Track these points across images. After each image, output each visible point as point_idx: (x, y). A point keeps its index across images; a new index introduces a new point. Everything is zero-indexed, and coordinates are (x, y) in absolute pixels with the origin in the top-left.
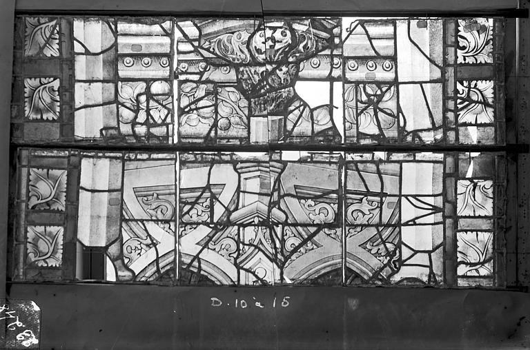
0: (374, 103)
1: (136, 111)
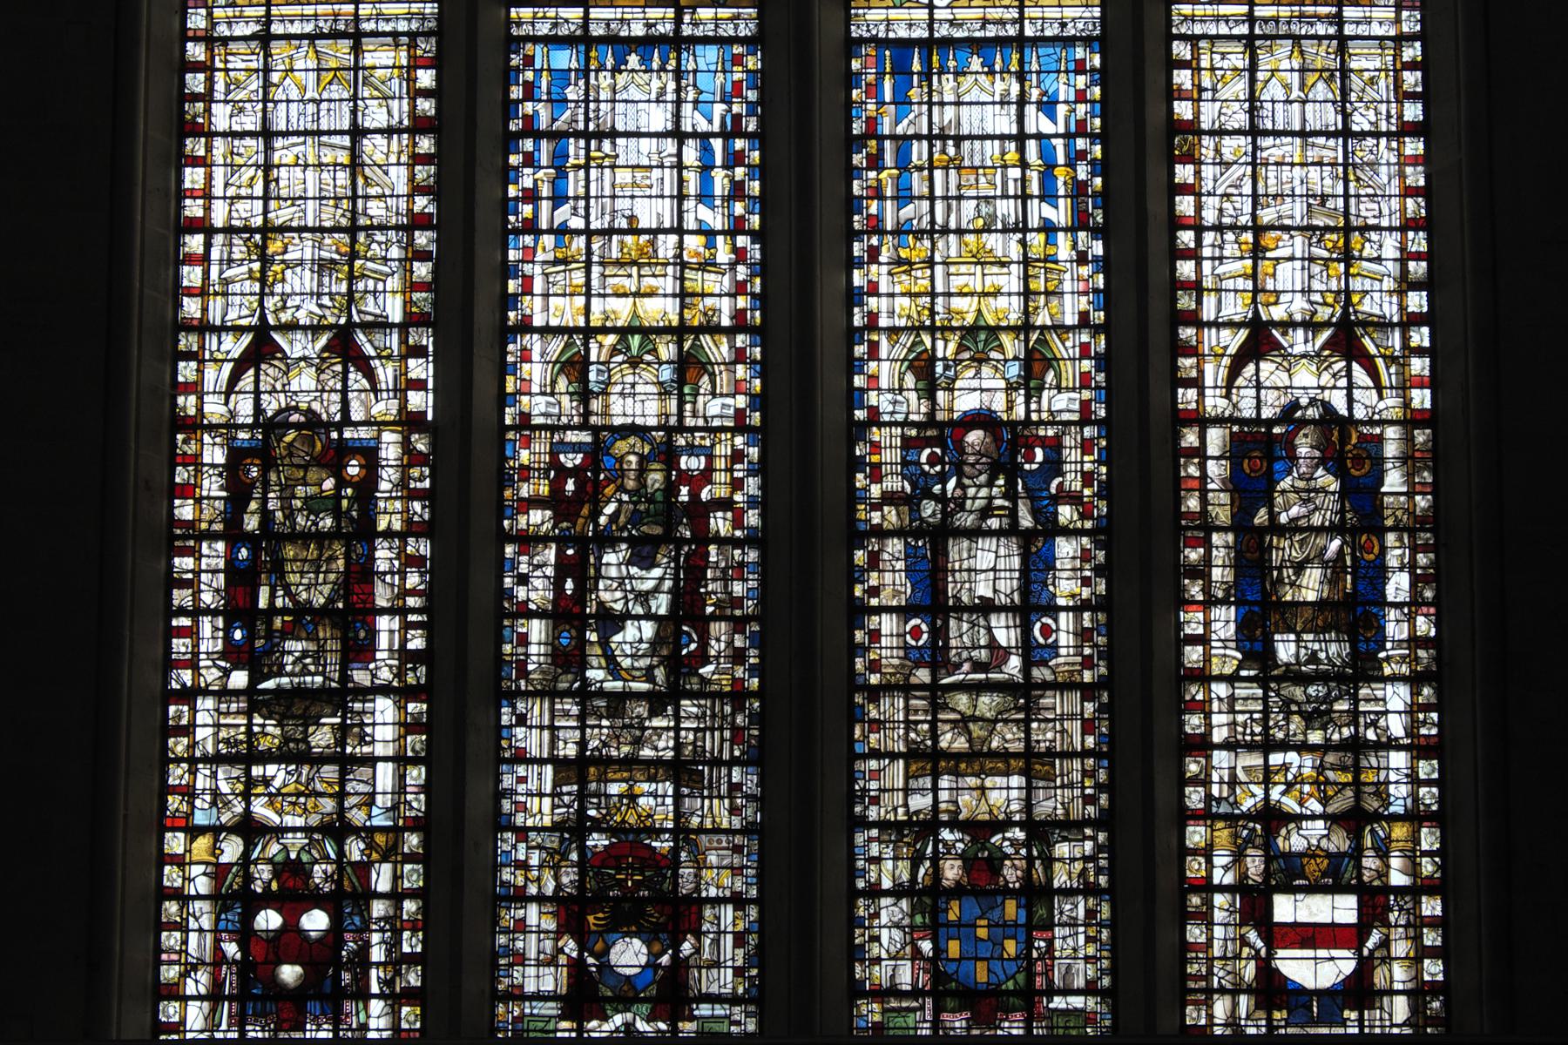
0: (1374, 724)
1: (1245, 729)
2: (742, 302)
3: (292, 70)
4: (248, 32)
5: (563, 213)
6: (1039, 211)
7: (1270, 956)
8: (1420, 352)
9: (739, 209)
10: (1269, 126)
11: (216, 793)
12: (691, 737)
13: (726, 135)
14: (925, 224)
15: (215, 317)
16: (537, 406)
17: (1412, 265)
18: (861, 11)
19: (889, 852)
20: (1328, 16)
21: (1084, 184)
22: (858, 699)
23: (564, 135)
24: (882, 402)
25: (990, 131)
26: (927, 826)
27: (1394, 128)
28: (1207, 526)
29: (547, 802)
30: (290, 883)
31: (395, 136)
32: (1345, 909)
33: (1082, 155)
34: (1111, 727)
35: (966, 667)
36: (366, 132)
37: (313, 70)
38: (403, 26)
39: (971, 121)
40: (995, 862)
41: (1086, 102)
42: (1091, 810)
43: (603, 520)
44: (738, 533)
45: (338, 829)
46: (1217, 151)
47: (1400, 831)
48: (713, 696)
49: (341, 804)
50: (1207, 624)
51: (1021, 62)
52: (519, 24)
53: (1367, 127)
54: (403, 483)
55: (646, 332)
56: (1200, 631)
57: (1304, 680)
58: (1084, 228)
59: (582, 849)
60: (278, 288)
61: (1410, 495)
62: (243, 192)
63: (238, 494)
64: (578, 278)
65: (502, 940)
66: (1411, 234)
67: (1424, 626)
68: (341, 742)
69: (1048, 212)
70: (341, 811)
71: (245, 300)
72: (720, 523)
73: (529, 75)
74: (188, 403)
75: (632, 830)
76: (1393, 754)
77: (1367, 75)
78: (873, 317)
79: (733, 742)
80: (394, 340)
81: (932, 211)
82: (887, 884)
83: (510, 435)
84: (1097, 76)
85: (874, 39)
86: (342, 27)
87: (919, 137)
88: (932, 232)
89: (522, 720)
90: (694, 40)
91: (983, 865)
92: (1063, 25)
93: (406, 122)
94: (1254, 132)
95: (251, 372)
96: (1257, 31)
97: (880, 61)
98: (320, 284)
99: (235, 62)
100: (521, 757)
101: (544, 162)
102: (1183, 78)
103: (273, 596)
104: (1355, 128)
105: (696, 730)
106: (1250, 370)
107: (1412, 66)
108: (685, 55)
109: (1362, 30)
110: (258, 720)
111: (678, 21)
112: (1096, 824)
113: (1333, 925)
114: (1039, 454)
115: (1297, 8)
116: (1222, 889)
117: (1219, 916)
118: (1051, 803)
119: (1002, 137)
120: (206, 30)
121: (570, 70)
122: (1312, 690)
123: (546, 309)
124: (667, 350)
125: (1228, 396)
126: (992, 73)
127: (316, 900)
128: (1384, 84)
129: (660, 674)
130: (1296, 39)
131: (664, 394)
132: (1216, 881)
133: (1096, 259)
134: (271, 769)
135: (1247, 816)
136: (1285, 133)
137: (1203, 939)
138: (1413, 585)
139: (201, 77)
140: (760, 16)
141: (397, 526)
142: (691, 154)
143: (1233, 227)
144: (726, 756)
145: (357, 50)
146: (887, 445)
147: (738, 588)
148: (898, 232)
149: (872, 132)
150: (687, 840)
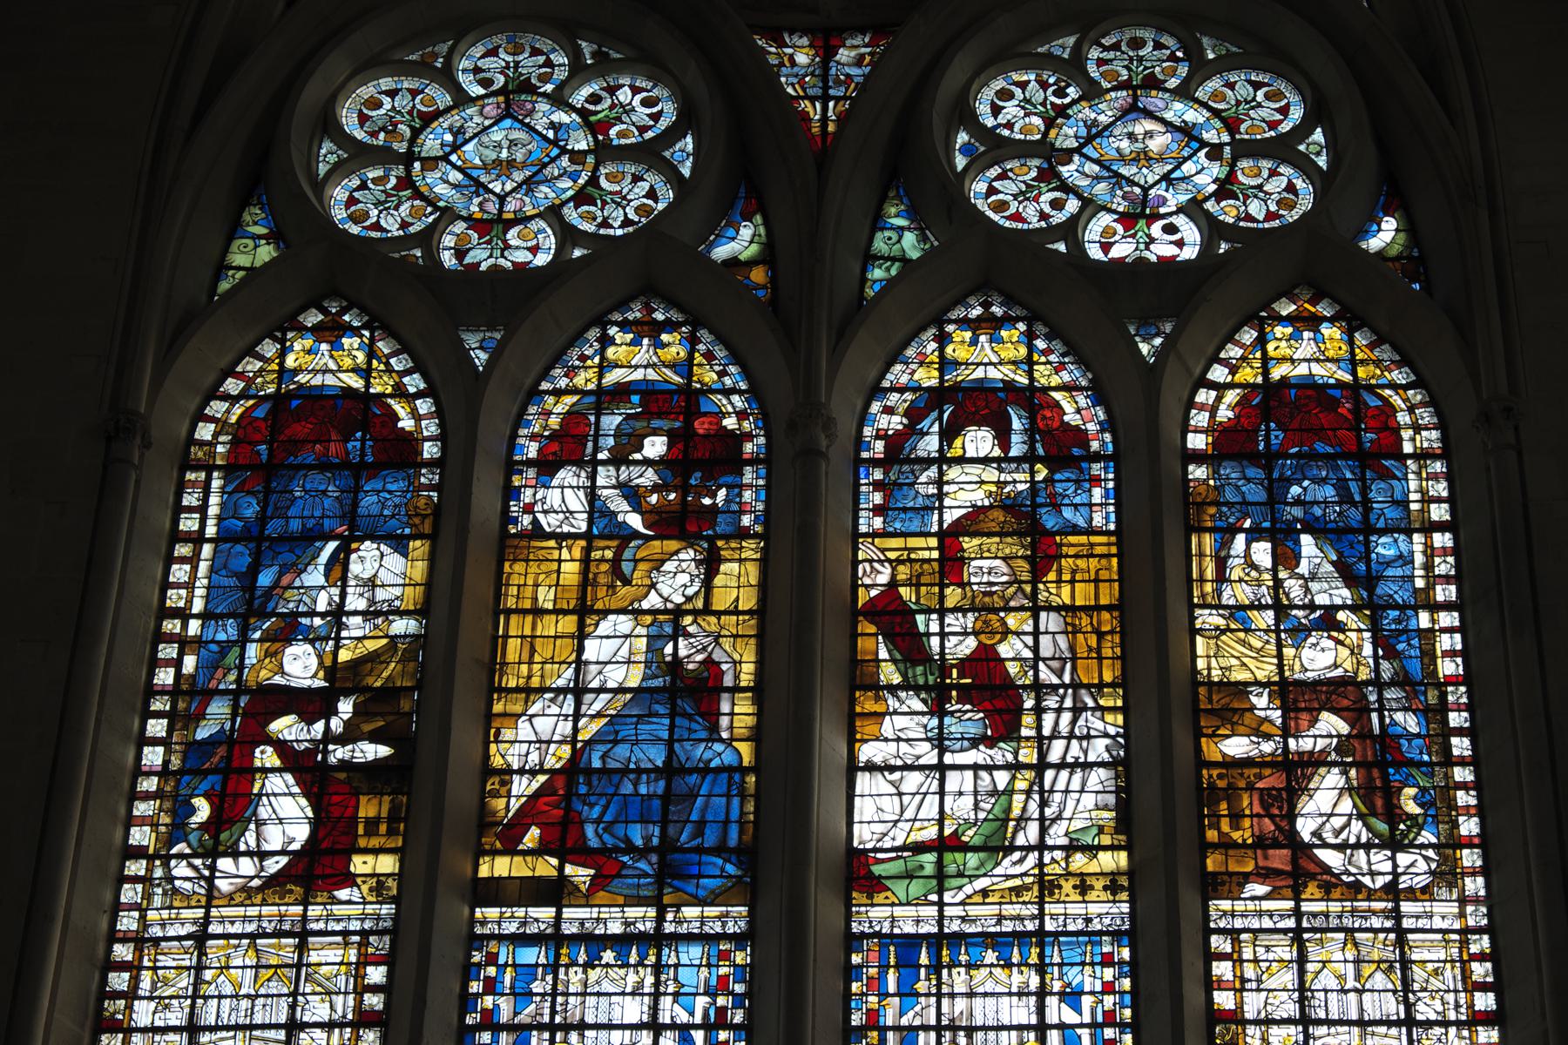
3: (228, 967)
4: (183, 932)
10: (1322, 1015)
13: (706, 1026)
18: (863, 909)
20: (1383, 911)
23: (529, 1027)
25: (1006, 1022)
27: (1464, 1018)
31: (337, 1031)
36: (304, 1026)
37: (251, 967)
38: (355, 925)
39: (983, 1012)
41: (1114, 992)
51: (1041, 956)
52: (484, 923)
53: (1433, 1017)
73: (492, 971)
77: (1430, 967)
84: (1126, 969)
85: (878, 935)
86: (287, 927)
87: (926, 1028)
90: (677, 938)
92: (1088, 920)
93: (350, 1016)
96: (1305, 924)
97: (883, 954)
99: (164, 961)
102: (1222, 969)
104: (1419, 1017)
107: (1481, 957)
108: (666, 951)
111: (660, 919)
115: (1349, 904)
119: (1020, 1028)
120: (137, 932)
121: (537, 965)
126: (1008, 965)
128: (1451, 975)
136: (1341, 1022)
139: (126, 976)
140: (751, 913)
145: (302, 948)
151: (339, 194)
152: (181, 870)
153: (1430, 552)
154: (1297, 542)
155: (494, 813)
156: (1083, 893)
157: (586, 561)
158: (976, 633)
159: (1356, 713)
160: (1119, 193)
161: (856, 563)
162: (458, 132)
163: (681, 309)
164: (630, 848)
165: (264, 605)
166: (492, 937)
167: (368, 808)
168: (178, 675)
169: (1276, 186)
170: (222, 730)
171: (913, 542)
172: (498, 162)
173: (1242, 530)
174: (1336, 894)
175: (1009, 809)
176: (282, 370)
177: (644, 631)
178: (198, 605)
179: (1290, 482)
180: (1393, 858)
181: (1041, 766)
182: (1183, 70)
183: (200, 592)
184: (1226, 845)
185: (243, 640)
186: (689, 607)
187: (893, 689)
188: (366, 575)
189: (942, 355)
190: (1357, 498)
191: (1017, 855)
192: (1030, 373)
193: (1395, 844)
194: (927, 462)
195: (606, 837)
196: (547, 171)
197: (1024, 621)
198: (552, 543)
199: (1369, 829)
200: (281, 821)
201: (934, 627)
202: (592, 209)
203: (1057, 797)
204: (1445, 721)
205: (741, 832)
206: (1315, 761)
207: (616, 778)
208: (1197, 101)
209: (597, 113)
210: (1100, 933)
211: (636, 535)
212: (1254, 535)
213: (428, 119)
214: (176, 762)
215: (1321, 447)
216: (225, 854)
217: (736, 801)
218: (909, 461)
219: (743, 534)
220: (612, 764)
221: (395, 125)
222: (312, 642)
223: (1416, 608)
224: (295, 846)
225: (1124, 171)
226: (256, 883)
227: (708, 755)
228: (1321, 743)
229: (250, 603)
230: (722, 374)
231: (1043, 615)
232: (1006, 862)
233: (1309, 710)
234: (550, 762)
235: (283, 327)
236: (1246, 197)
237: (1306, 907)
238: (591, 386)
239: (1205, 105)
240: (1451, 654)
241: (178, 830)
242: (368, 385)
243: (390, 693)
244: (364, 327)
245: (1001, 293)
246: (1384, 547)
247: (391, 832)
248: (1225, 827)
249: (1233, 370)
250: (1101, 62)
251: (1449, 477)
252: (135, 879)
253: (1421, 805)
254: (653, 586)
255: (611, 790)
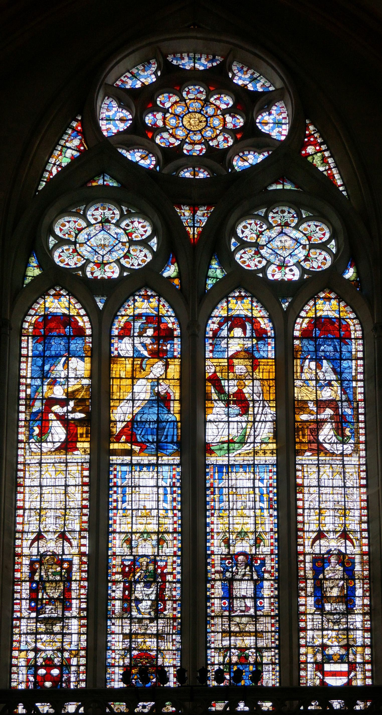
0: (352, 624)
2: (175, 526)
5: (125, 505)
6: (258, 505)
7: (323, 679)
8: (365, 538)
9: (175, 504)
10: (323, 485)
11: (27, 642)
12: (161, 628)
13: (170, 486)
14: (227, 507)
15: (26, 529)
16: (118, 551)
17: (363, 518)
19: (217, 655)
21: (272, 498)
22: (208, 619)
23: (126, 487)
24: (215, 550)
26: (228, 649)
28: (306, 579)
29: (121, 643)
30: (48, 663)
32: (344, 667)
33: (271, 492)
34: (279, 625)
35: (239, 611)
36: (69, 486)
38: (79, 461)
39: (240, 484)
40: (247, 657)
42: (273, 645)
43: (136, 577)
44: (174, 580)
45: (62, 650)
46: (309, 491)
47: (360, 649)
48: (167, 618)
49: (62, 644)
50: (306, 601)
51: (254, 470)
52: (112, 460)
53: (350, 486)
54: (80, 568)
55: (148, 533)
56: (304, 603)
57: (333, 614)
58: (272, 508)
59: (131, 655)
60: (44, 522)
61: (363, 571)
62: (34, 500)
63: (33, 571)
64: (130, 520)
65: (108, 676)
66: (363, 511)
67: (366, 602)
68: (63, 630)
69: (261, 505)
70: (62, 646)
71: (35, 525)
72: (169, 578)
73: (115, 472)
74: (18, 550)
75: (144, 650)
76: (357, 631)
78: (212, 530)
79: (173, 629)
80: (77, 535)
81: (229, 505)
82: (216, 662)
83: (110, 557)
85: (213, 464)
86: (62, 461)
87: (225, 487)
88: (229, 509)
89: (113, 624)
90: (162, 465)
91: (243, 659)
92: (266, 461)
93: (80, 483)
94: (319, 486)
95: (37, 542)
98: (56, 521)
99: (31, 469)
100: (113, 633)
101: (119, 492)
103: (43, 595)
105: (163, 626)
106: (318, 542)
107: (363, 471)
109: (349, 463)
110: (38, 624)
111: (158, 460)
112: (275, 648)
113: (341, 671)
114: (259, 562)
116: (310, 663)
117: (309, 669)
118: (262, 643)
119: (249, 488)
122: (335, 617)
123: (120, 527)
124: (154, 537)
125: (312, 548)
126: (246, 472)
127: (55, 666)
129: (152, 613)
130: (331, 464)
131: (153, 547)
132: (308, 661)
133: (275, 516)
134: (42, 636)
135: (317, 646)
136: (328, 487)
137: (305, 675)
138: (363, 592)
139: (22, 473)
140: (180, 459)
141: (78, 579)
142: (161, 491)
143: (313, 509)
144: (171, 632)
145: (66, 466)
146: (217, 559)
147: (174, 593)
148: (219, 509)
149: (212, 486)
150: (160, 652)
151: (56, 254)
152: (33, 446)
153: (357, 365)
154: (322, 362)
155: (113, 432)
156: (265, 454)
157: (133, 364)
158: (237, 386)
159: (336, 409)
160: (277, 259)
161: (205, 366)
162: (89, 235)
163: (155, 291)
164: (149, 442)
165: (47, 375)
166: (115, 464)
167: (80, 430)
168: (26, 394)
169: (321, 258)
170: (39, 409)
171: (220, 360)
172: (101, 245)
173: (307, 359)
174: (328, 455)
175: (246, 433)
176: (45, 308)
177: (149, 384)
178: (29, 375)
179: (321, 345)
180: (343, 446)
181: (254, 422)
182: (296, 221)
183: (29, 371)
184: (301, 442)
185: (43, 385)
186: (161, 377)
187: (215, 400)
188: (74, 367)
189: (228, 307)
190: (339, 350)
191: (248, 444)
192: (252, 312)
193: (343, 443)
194: (224, 338)
195: (142, 439)
196: (115, 248)
197: (250, 383)
198: (123, 359)
199: (337, 439)
200: (58, 434)
201: (226, 384)
202: (128, 260)
203: (258, 430)
204: (358, 411)
205: (177, 438)
206: (324, 421)
207: (144, 423)
208: (299, 231)
209: (128, 230)
210: (269, 464)
211: (146, 357)
212: (311, 360)
213: (80, 230)
214: (28, 418)
215: (330, 336)
216: (44, 442)
217: (175, 430)
218: (219, 337)
219: (175, 357)
220: (143, 420)
221: (70, 232)
222: (61, 385)
223: (352, 381)
224: (62, 440)
225: (279, 252)
226: (53, 450)
227: (168, 418)
228: (326, 417)
229: (43, 374)
230: (167, 311)
231: (255, 381)
232: (245, 446)
233: (323, 408)
234: (127, 419)
235: (44, 294)
236: (312, 261)
237: (320, 458)
238: (132, 314)
239: (302, 232)
240: (360, 393)
241: (30, 436)
242: (69, 312)
243: (83, 400)
244: (67, 295)
245: (244, 288)
246: (345, 364)
247: (87, 437)
248: (301, 438)
249: (307, 313)
250: (273, 217)
251: (363, 345)
252: (21, 448)
253: (351, 433)
254: (151, 371)
255: (143, 427)
